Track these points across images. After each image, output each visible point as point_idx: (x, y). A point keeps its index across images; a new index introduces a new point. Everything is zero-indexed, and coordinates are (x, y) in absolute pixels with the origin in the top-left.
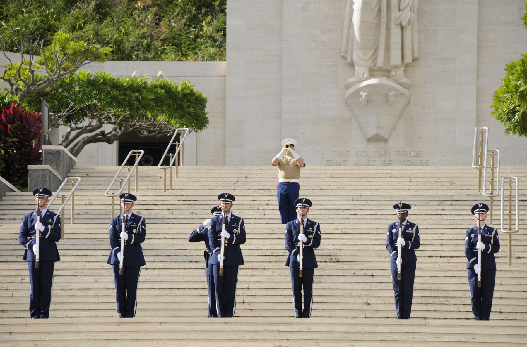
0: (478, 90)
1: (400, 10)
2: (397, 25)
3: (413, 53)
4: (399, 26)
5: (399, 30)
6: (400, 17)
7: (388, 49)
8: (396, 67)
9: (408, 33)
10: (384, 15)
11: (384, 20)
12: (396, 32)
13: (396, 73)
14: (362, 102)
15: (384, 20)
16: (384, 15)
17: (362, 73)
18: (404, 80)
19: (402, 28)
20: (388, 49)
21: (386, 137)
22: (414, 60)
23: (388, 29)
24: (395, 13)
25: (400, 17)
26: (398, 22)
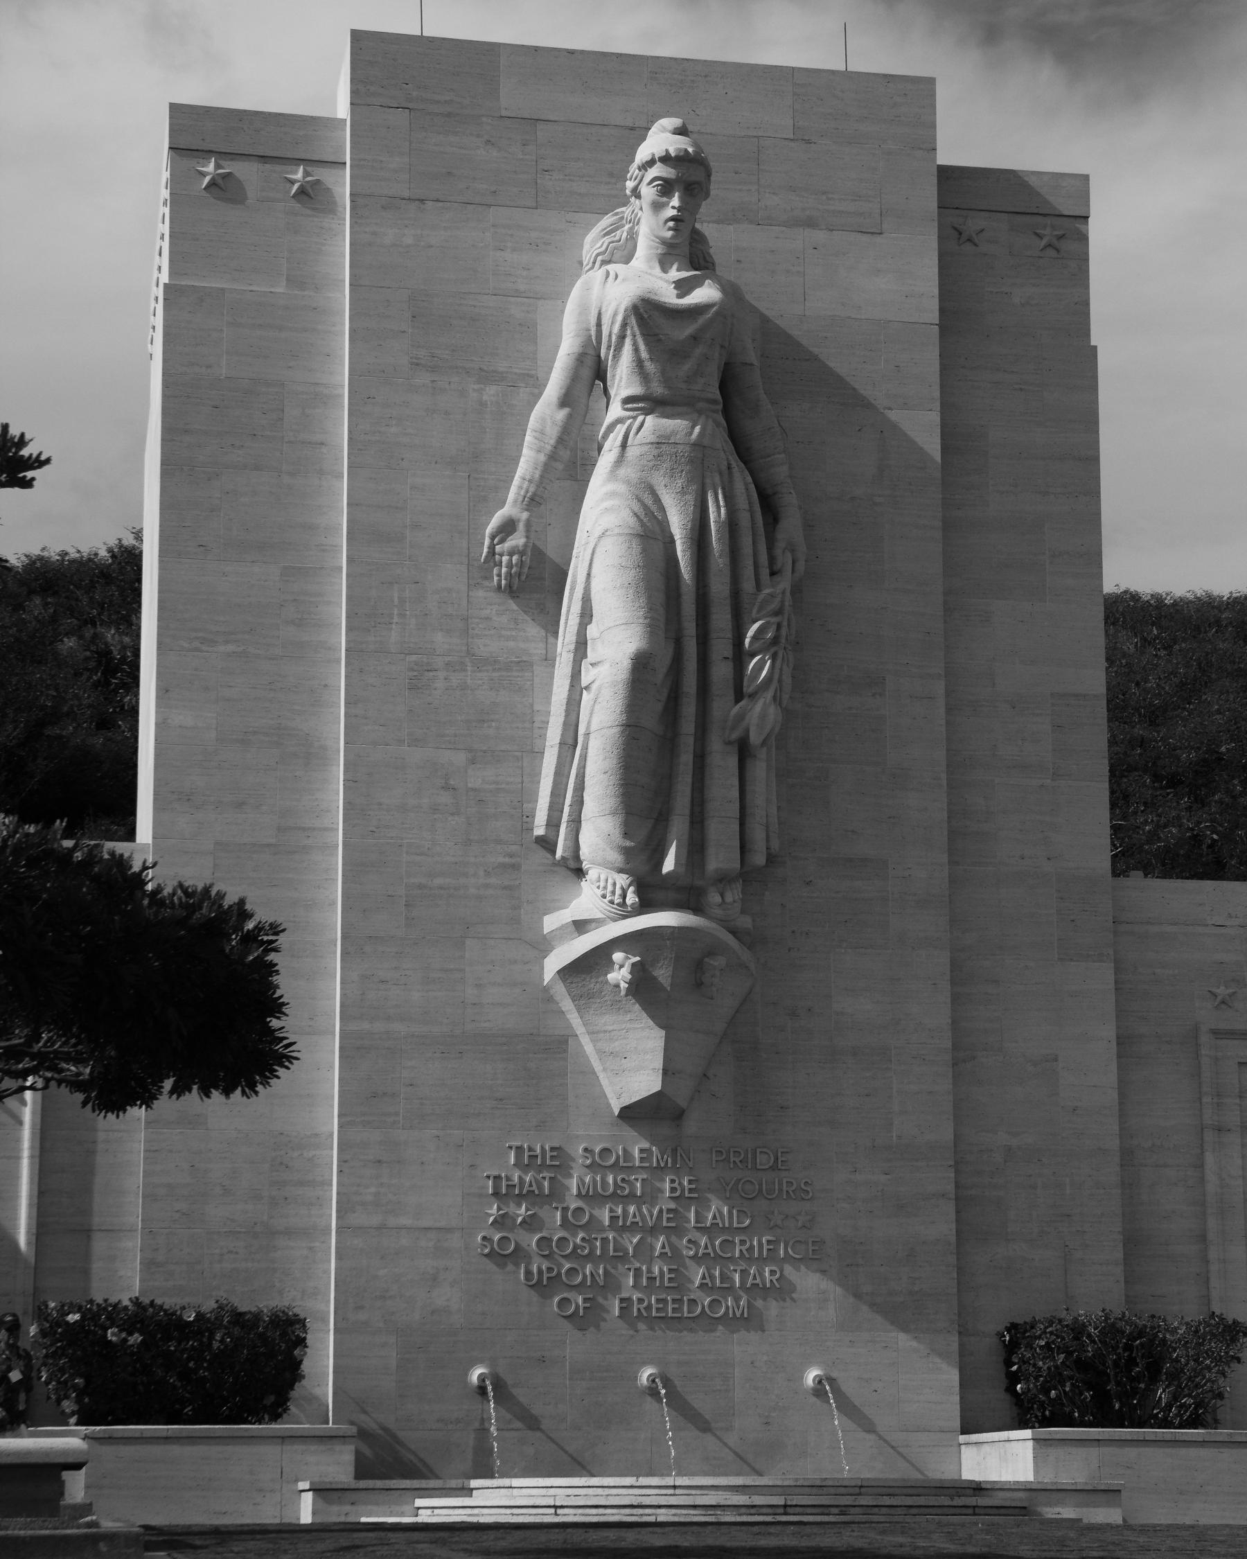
0: (955, 965)
1: (739, 695)
2: (729, 743)
3: (768, 840)
4: (735, 749)
5: (733, 761)
6: (741, 717)
7: (698, 820)
8: (723, 880)
9: (760, 770)
10: (689, 709)
11: (688, 727)
12: (723, 765)
13: (722, 896)
14: (617, 986)
15: (688, 727)
16: (689, 709)
17: (618, 891)
18: (745, 922)
19: (744, 750)
20: (698, 820)
21: (683, 1103)
22: (771, 859)
23: (701, 758)
24: (722, 706)
25: (741, 717)
26: (735, 735)
